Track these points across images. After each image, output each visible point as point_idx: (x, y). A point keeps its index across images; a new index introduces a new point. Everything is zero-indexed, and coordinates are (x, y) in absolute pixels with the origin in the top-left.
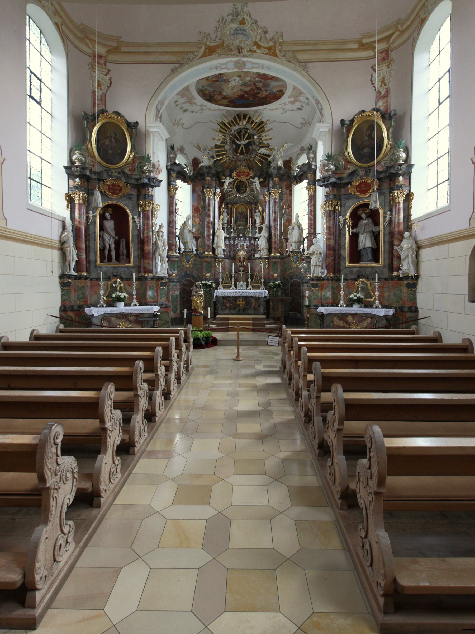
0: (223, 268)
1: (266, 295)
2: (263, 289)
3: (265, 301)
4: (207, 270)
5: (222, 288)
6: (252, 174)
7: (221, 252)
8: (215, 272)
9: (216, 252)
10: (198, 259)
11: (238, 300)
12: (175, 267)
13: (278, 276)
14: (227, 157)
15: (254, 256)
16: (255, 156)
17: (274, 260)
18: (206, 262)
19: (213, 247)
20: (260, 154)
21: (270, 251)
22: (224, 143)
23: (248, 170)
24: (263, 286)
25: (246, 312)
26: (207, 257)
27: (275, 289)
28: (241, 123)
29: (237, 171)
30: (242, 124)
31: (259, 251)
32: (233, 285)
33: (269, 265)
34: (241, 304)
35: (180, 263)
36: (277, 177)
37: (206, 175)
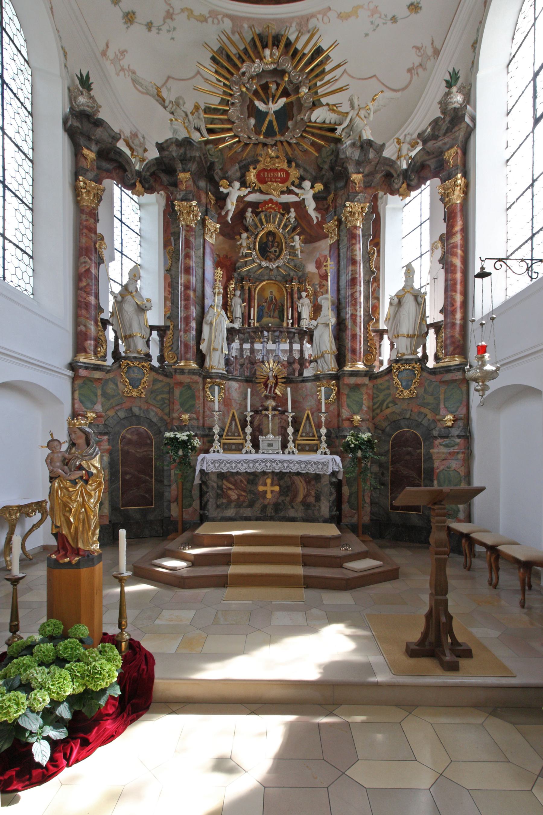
0: (226, 402)
1: (336, 469)
2: (325, 454)
3: (332, 484)
4: (182, 405)
5: (221, 451)
6: (294, 173)
7: (219, 363)
8: (204, 412)
9: (207, 364)
10: (161, 378)
11: (261, 481)
12: (96, 396)
13: (363, 420)
14: (235, 136)
15: (301, 374)
16: (301, 136)
17: (352, 380)
18: (181, 384)
19: (199, 351)
20: (315, 122)
21: (341, 360)
22: (227, 103)
23: (285, 166)
24: (324, 445)
25: (282, 514)
26: (182, 371)
27: (359, 454)
28: (267, 52)
29: (260, 167)
30: (271, 56)
31: (311, 362)
32: (249, 441)
33: (338, 393)
34: (269, 492)
35: (115, 387)
36: (359, 173)
37: (179, 166)
